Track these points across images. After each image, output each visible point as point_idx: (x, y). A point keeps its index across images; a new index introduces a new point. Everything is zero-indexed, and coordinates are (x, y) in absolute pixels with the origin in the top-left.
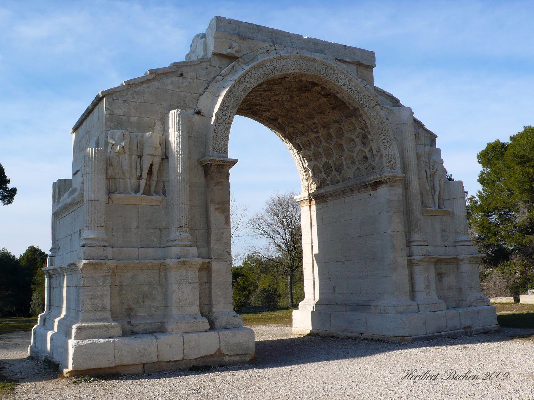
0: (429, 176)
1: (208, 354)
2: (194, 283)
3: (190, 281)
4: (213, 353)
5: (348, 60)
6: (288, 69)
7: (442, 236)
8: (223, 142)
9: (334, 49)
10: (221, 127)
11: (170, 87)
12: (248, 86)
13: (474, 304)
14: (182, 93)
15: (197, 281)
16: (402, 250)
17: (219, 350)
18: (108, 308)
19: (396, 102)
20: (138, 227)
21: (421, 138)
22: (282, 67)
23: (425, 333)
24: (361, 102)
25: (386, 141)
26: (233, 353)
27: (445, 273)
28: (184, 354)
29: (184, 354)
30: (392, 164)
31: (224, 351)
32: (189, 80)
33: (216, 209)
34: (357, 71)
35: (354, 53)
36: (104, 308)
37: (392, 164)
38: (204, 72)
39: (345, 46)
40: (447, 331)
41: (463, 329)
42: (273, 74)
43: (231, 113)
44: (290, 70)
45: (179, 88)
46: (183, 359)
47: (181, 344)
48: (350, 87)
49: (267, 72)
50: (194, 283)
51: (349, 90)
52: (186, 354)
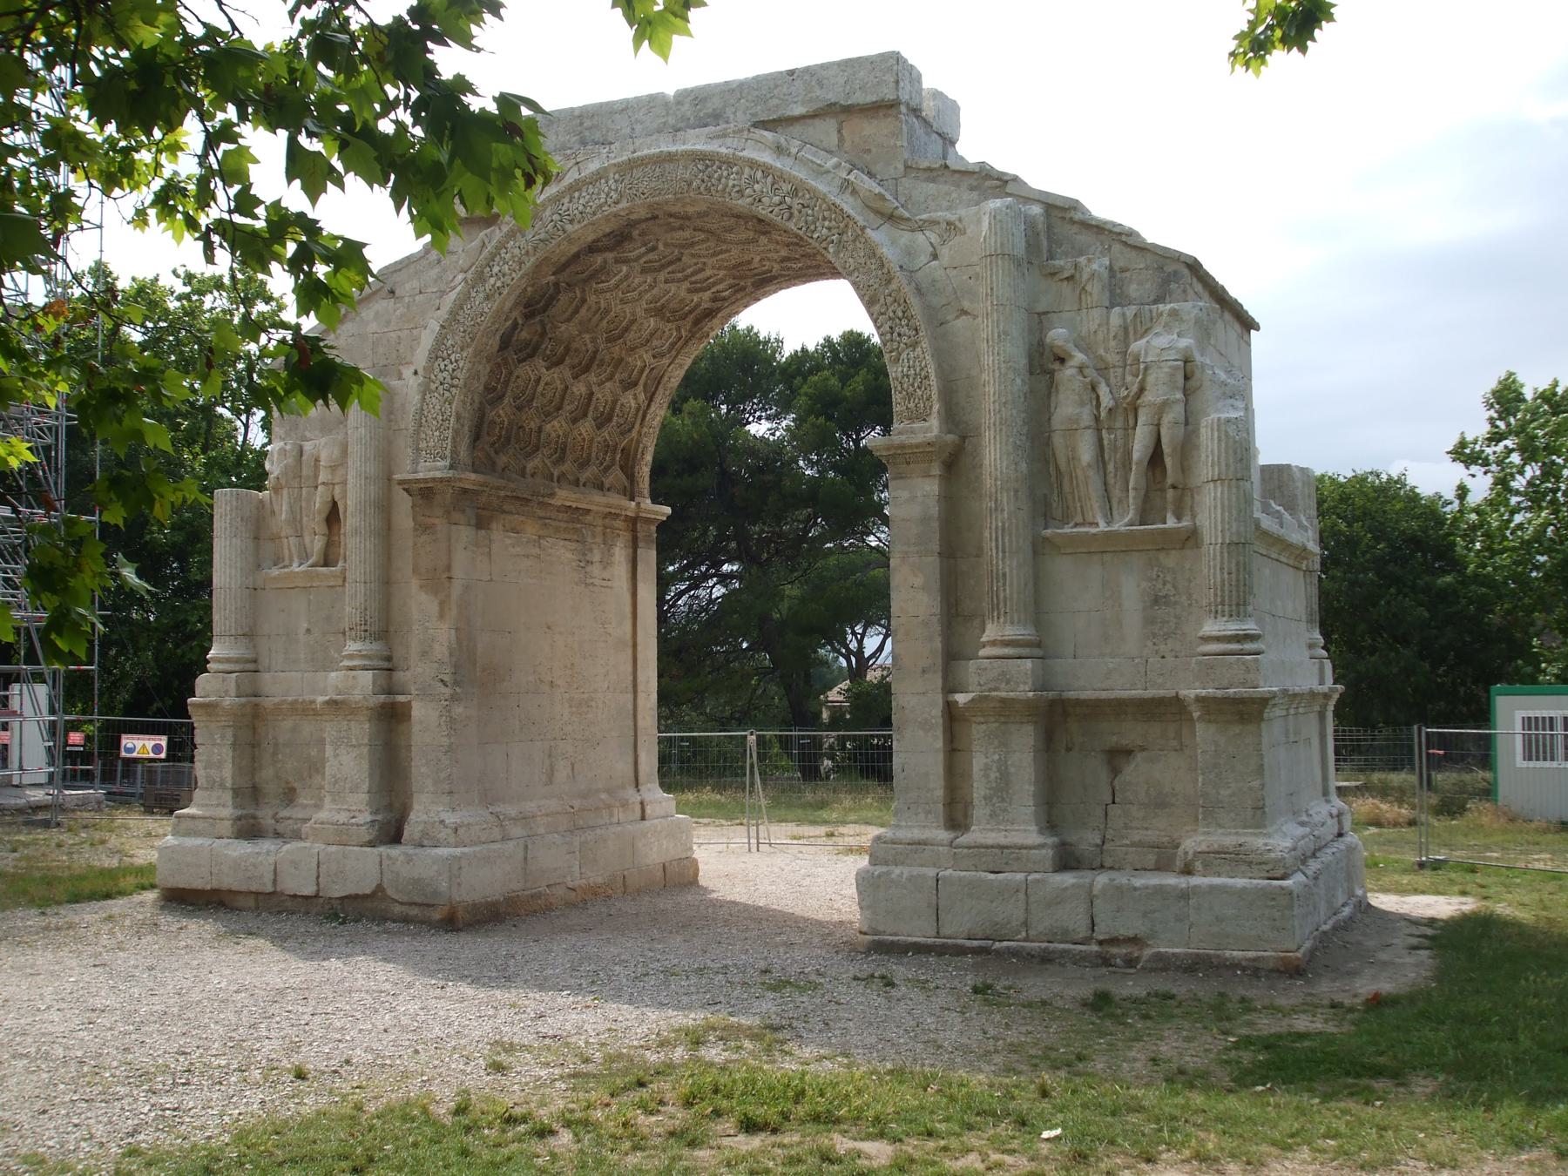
0: (1103, 414)
1: (360, 893)
2: (360, 745)
3: (354, 742)
4: (368, 891)
5: (799, 110)
6: (601, 206)
7: (1149, 621)
8: (437, 433)
9: (756, 93)
10: (434, 399)
11: (373, 327)
12: (499, 284)
13: (1198, 865)
14: (392, 334)
15: (366, 741)
16: (924, 671)
17: (380, 888)
18: (229, 784)
19: (998, 183)
20: (308, 631)
21: (1088, 288)
22: (581, 208)
23: (934, 933)
24: (815, 236)
25: (895, 334)
26: (405, 899)
27: (1143, 749)
28: (318, 884)
29: (318, 884)
30: (912, 405)
31: (390, 892)
32: (406, 300)
33: (421, 587)
34: (839, 131)
35: (820, 84)
36: (222, 786)
37: (912, 405)
38: (434, 273)
39: (791, 73)
40: (1026, 939)
41: (1101, 943)
42: (560, 233)
43: (456, 361)
44: (606, 208)
45: (388, 323)
46: (317, 896)
47: (314, 865)
48: (776, 199)
49: (542, 236)
50: (360, 745)
51: (777, 209)
52: (322, 886)
